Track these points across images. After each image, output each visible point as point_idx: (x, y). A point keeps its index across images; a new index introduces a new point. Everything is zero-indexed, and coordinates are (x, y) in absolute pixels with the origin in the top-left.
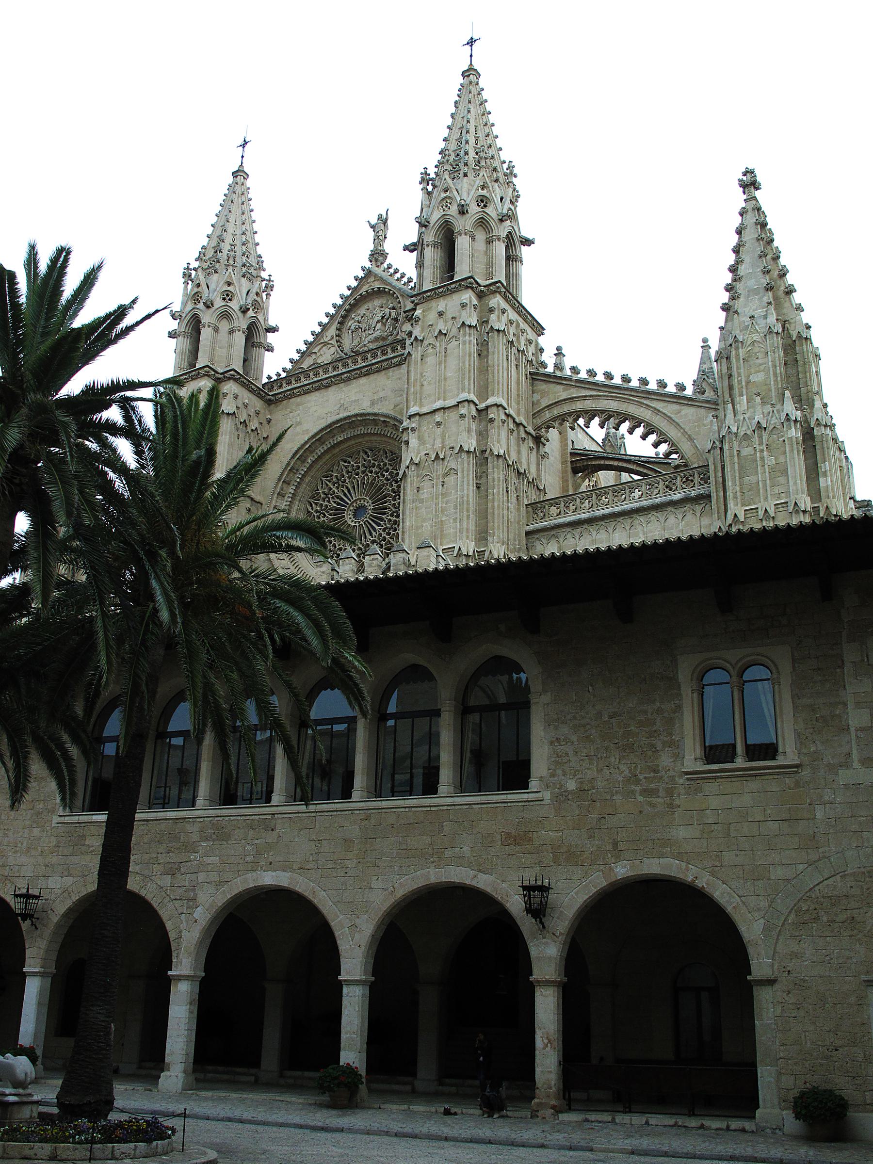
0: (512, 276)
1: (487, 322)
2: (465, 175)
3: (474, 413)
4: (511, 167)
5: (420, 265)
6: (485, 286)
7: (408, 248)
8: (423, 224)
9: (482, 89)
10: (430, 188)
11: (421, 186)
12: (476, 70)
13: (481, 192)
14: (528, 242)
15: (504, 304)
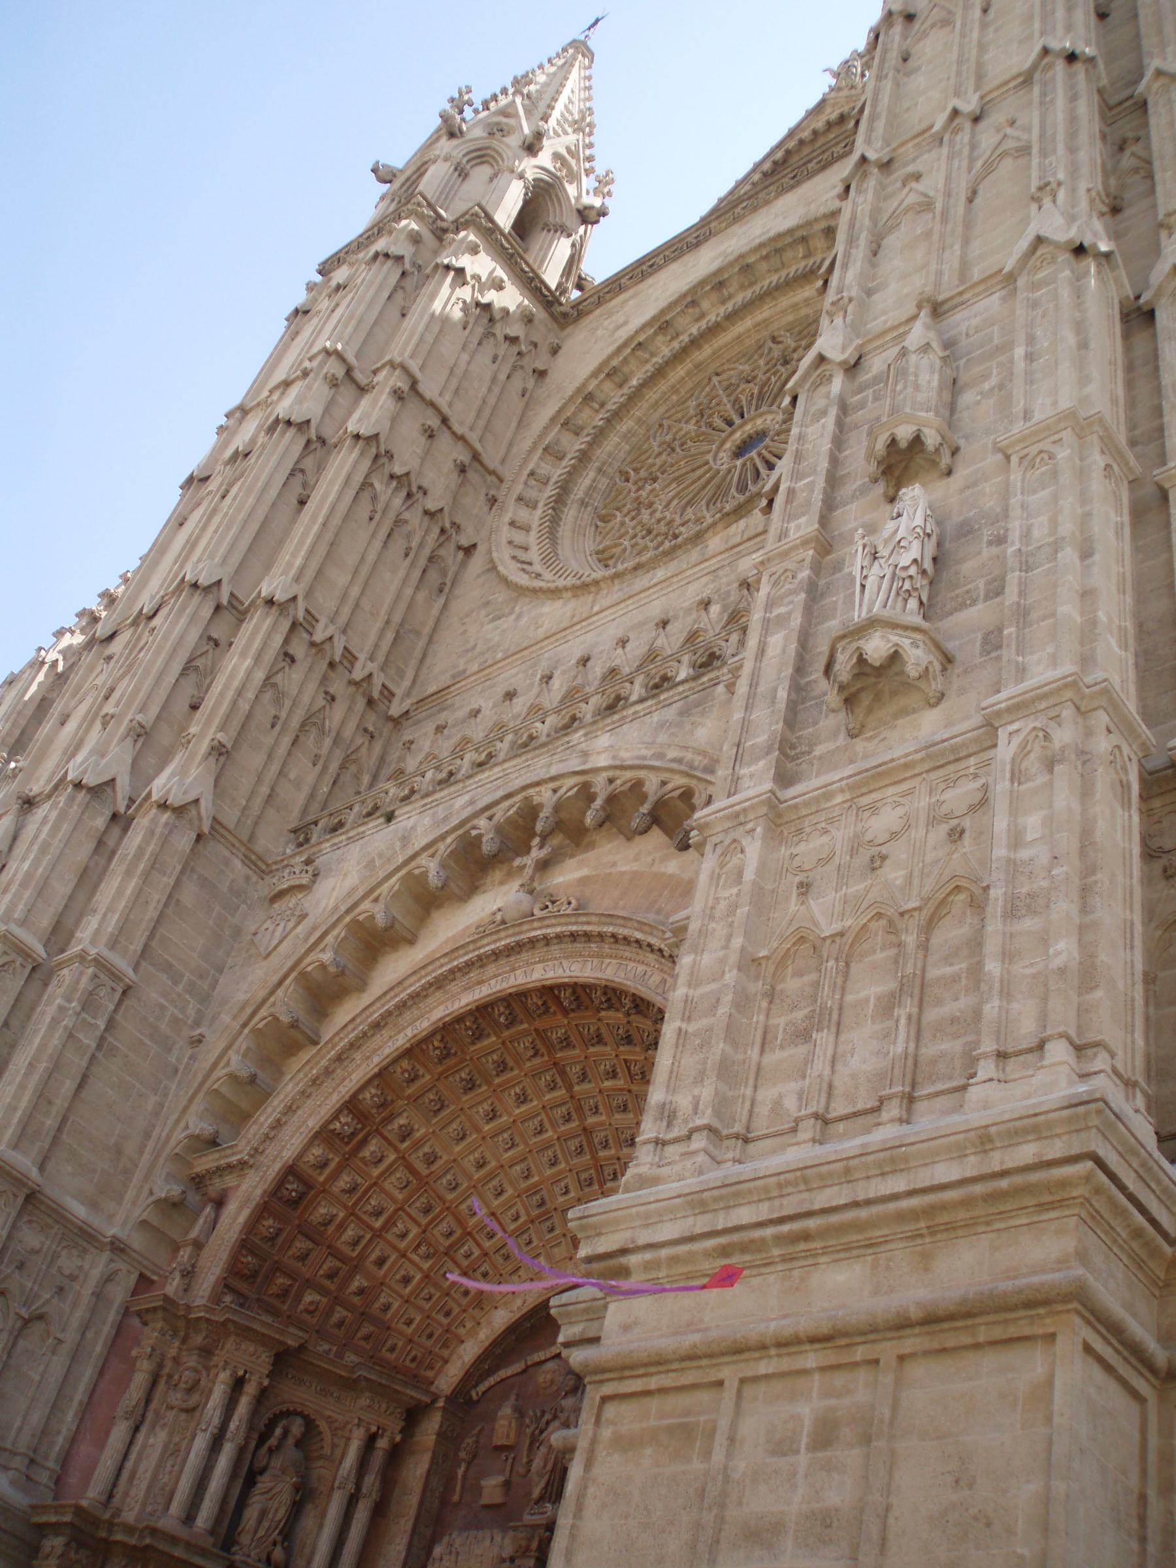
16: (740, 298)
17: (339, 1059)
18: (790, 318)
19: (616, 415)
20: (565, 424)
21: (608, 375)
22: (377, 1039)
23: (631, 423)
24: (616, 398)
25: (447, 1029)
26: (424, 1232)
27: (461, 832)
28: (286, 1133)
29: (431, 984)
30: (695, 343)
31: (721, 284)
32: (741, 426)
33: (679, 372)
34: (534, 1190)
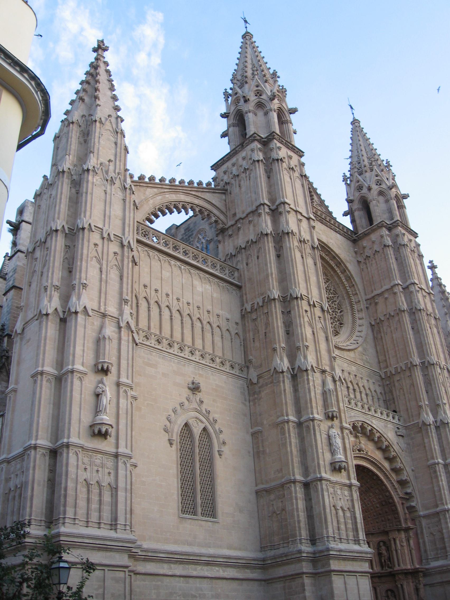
0: (403, 215)
1: (396, 242)
2: (366, 171)
3: (401, 290)
4: (388, 162)
5: (353, 221)
6: (391, 224)
7: (345, 214)
8: (349, 201)
9: (363, 128)
10: (348, 182)
11: (344, 182)
12: (357, 120)
13: (377, 178)
14: (406, 196)
15: (403, 231)
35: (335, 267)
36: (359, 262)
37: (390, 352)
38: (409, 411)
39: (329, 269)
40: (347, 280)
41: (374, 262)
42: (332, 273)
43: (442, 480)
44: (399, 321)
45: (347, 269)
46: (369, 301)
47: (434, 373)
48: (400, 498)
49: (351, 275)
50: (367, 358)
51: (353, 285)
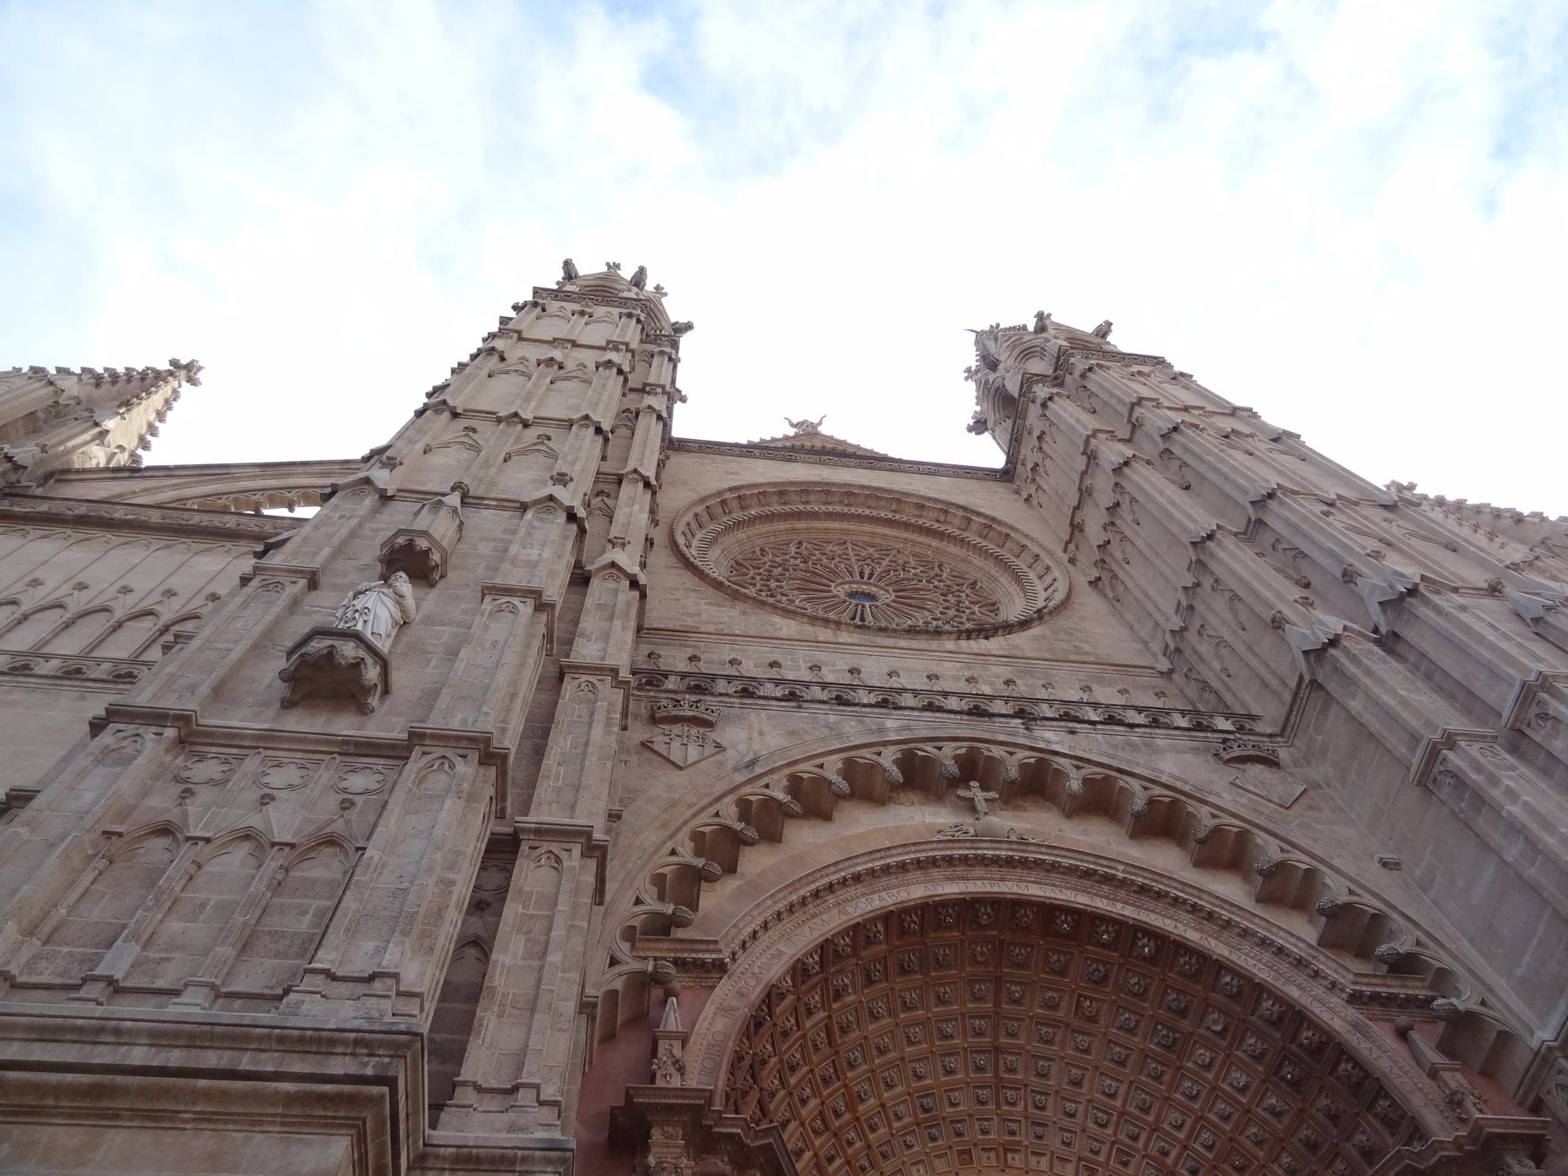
14: (1104, 330)
16: (838, 509)
17: (816, 894)
18: (867, 539)
19: (739, 524)
20: (708, 507)
21: (739, 496)
22: (851, 891)
23: (744, 536)
24: (738, 515)
25: (931, 911)
26: (823, 1103)
27: (904, 747)
28: (757, 947)
29: (918, 861)
30: (799, 515)
31: (828, 493)
32: (866, 584)
33: (782, 526)
34: (926, 1093)
35: (936, 525)
36: (1028, 500)
37: (1152, 592)
38: (1268, 677)
39: (923, 539)
40: (985, 537)
41: (1048, 462)
42: (935, 543)
43: (1512, 795)
44: (1133, 500)
45: (973, 512)
46: (1071, 547)
47: (1286, 513)
48: (1355, 999)
49: (993, 519)
50: (1075, 646)
51: (1007, 535)
